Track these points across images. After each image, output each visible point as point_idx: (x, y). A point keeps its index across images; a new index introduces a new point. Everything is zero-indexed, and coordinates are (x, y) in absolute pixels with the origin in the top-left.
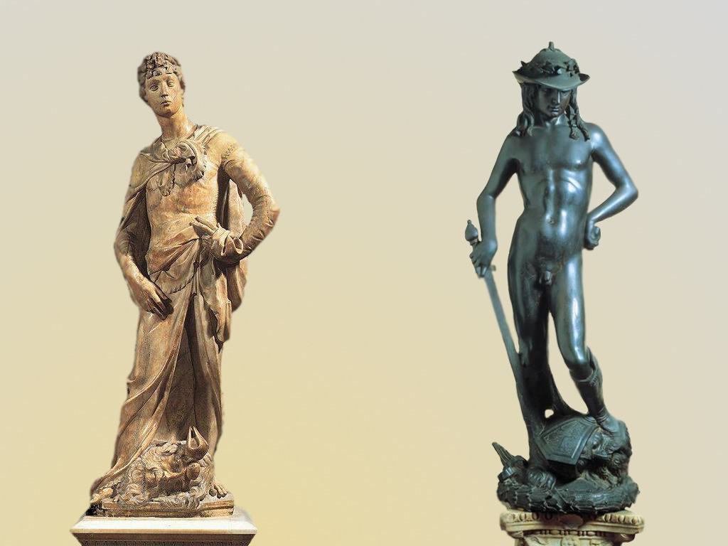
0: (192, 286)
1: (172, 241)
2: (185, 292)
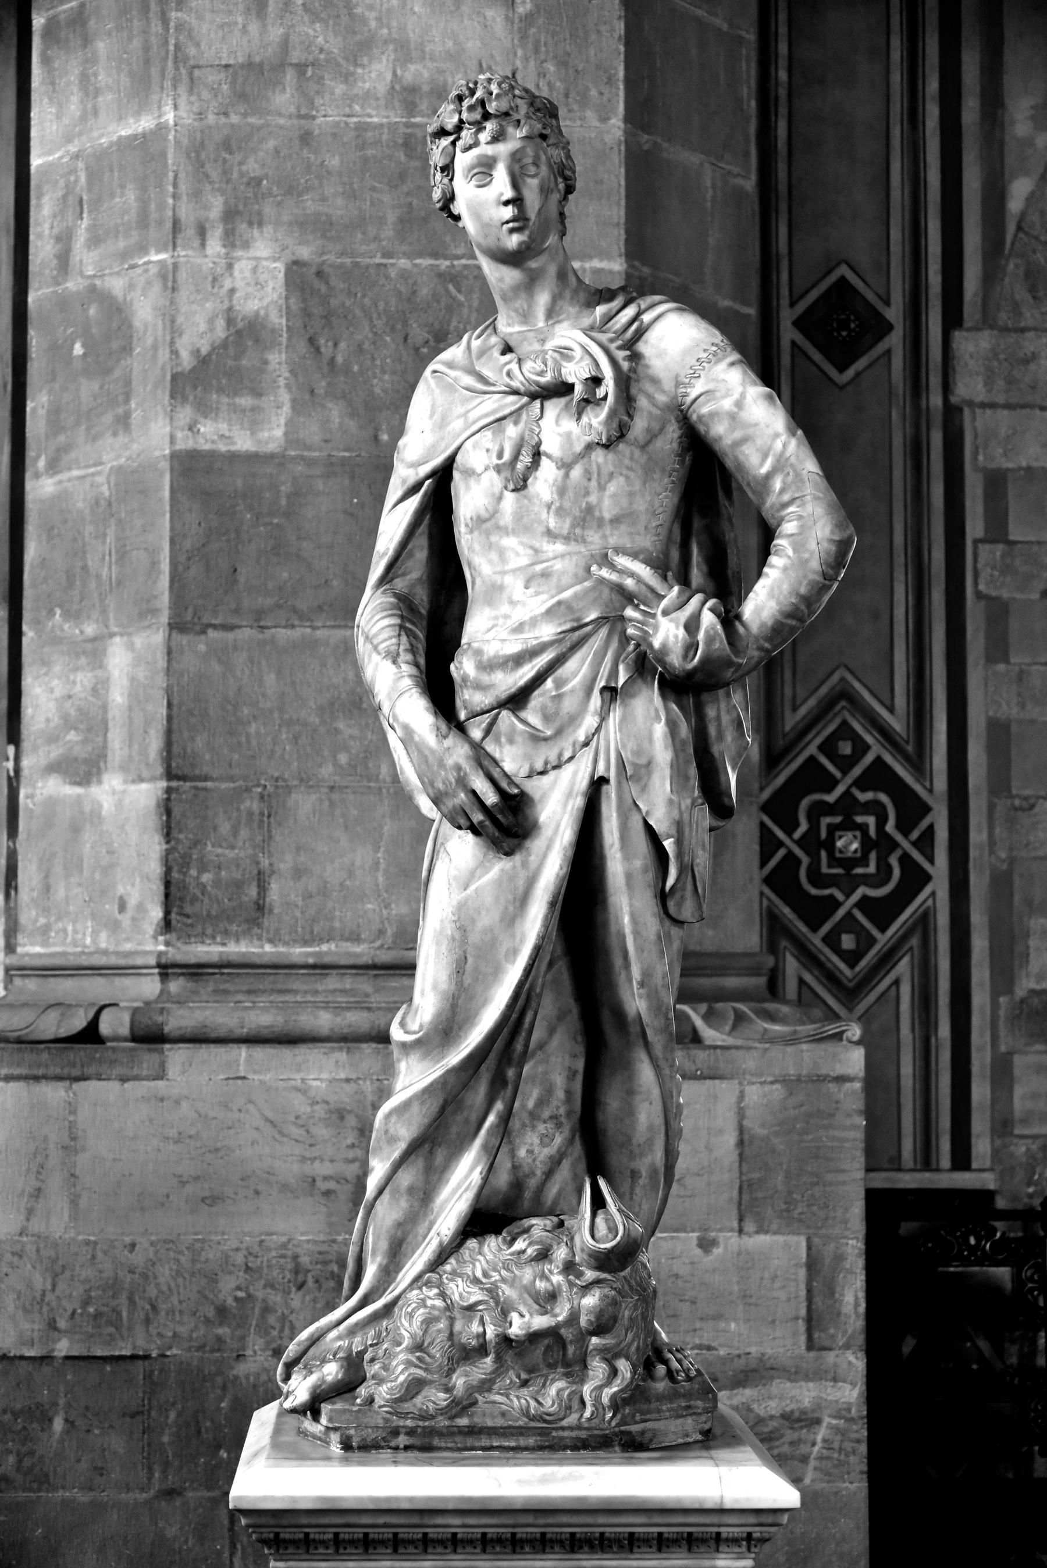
0: (596, 754)
1: (534, 622)
2: (575, 778)
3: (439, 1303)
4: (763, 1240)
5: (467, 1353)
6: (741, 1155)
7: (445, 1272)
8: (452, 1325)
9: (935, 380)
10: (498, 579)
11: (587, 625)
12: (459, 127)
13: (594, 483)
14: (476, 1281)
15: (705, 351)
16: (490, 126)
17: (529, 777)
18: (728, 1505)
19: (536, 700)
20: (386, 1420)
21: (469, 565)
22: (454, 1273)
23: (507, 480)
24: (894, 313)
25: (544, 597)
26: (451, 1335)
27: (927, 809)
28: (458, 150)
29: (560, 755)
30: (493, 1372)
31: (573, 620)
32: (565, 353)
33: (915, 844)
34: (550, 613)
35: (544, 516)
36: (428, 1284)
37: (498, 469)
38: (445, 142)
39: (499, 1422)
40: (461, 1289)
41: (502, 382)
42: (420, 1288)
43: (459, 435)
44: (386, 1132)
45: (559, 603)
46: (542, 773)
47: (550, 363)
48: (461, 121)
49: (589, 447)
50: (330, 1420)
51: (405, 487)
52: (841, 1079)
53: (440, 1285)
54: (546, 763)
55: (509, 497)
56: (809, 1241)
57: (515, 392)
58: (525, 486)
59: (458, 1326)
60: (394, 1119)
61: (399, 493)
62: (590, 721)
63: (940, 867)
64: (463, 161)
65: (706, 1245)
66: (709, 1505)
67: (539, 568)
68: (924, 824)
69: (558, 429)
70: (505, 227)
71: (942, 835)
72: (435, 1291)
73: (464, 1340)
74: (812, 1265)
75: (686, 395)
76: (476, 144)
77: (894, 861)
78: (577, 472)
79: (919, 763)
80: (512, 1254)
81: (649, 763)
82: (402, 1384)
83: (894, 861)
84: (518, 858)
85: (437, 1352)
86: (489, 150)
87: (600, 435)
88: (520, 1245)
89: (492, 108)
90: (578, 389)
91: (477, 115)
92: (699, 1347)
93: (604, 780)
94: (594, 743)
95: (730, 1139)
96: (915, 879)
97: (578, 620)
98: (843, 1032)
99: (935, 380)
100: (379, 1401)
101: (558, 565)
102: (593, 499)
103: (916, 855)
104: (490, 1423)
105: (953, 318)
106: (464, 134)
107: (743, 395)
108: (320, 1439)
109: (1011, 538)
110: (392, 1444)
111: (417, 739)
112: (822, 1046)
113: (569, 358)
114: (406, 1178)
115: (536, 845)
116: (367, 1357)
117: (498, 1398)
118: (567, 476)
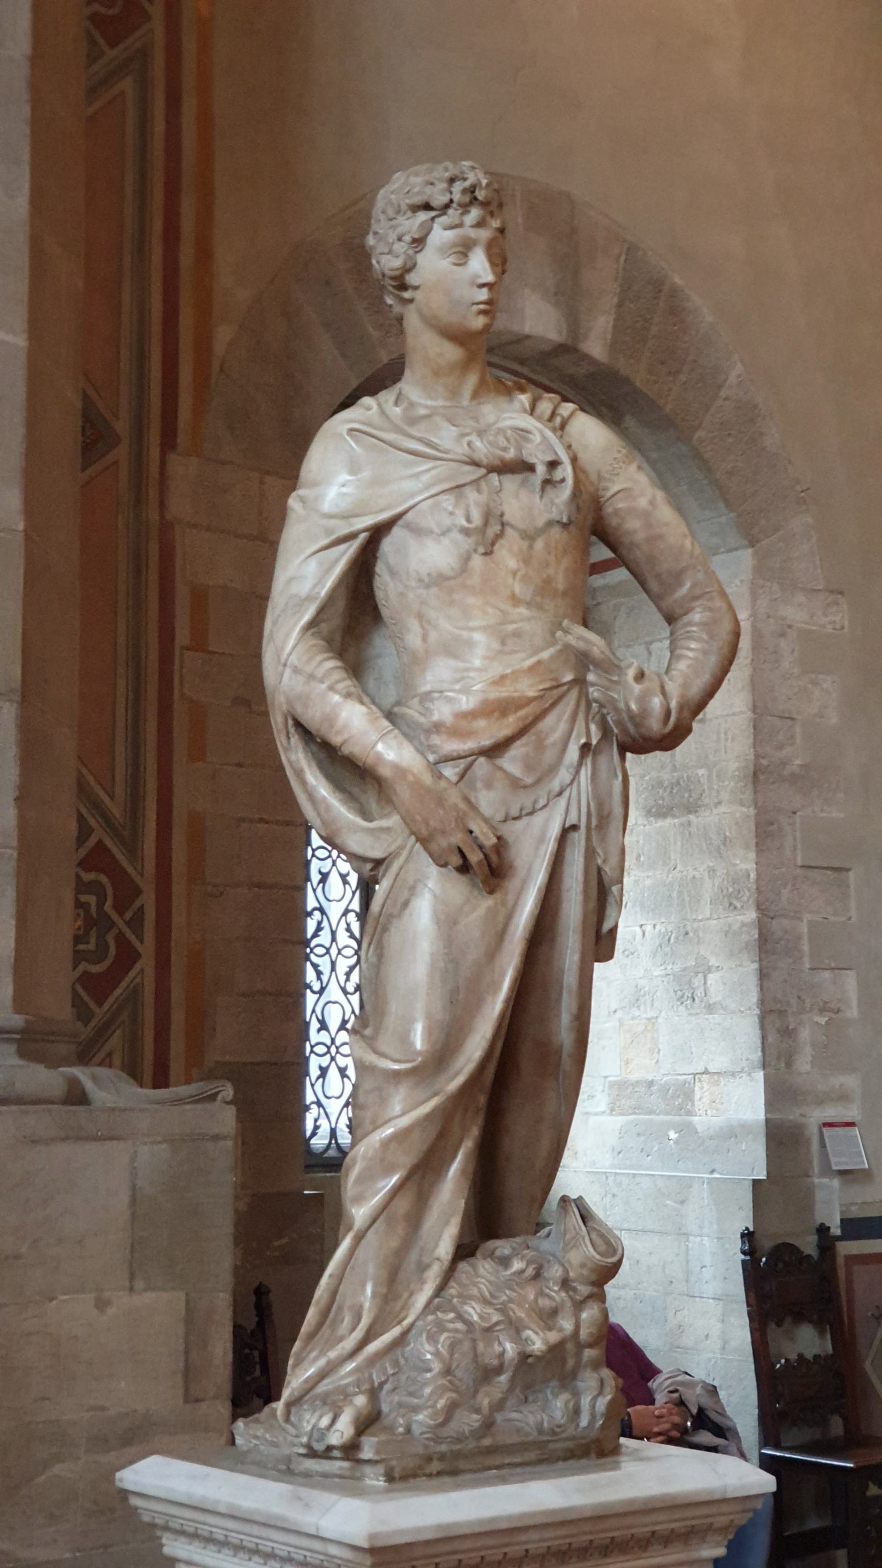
3: (459, 1326)
4: (149, 1297)
5: (487, 1374)
6: (134, 1216)
7: (453, 1297)
8: (474, 1348)
9: (153, 494)
10: (465, 634)
11: (565, 684)
12: (447, 206)
13: (552, 558)
14: (486, 1302)
15: (619, 452)
16: (475, 213)
17: (505, 821)
18: (730, 1495)
19: (518, 750)
20: (426, 1447)
21: (420, 617)
22: (465, 1298)
23: (478, 544)
24: (122, 426)
25: (522, 655)
26: (476, 1355)
27: (138, 892)
28: (437, 227)
29: (535, 802)
30: (507, 1391)
31: (551, 680)
32: (523, 433)
33: (128, 923)
34: (532, 669)
35: (510, 580)
36: (438, 1308)
37: (466, 532)
38: (423, 216)
39: (516, 1439)
40: (478, 1310)
41: (461, 450)
42: (433, 1313)
43: (413, 495)
44: (382, 1160)
45: (539, 662)
46: (515, 819)
47: (512, 441)
48: (451, 201)
49: (550, 524)
50: (378, 1452)
51: (334, 537)
52: (216, 1138)
53: (453, 1309)
54: (521, 810)
55: (477, 561)
56: (187, 1295)
57: (476, 464)
58: (491, 552)
59: (481, 1346)
60: (393, 1146)
61: (326, 541)
62: (564, 775)
63: (147, 947)
64: (440, 236)
65: (101, 1305)
66: (717, 1496)
67: (511, 628)
68: (137, 904)
69: (519, 502)
70: (475, 308)
71: (150, 915)
72: (452, 1315)
73: (487, 1361)
74: (189, 1319)
75: (606, 489)
76: (460, 225)
77: (110, 938)
78: (539, 545)
79: (132, 848)
80: (512, 1274)
81: (609, 815)
82: (442, 1408)
83: (110, 938)
84: (498, 895)
85: (464, 1374)
86: (473, 233)
87: (561, 513)
88: (517, 1265)
89: (481, 195)
90: (541, 469)
91: (467, 198)
92: (93, 1408)
93: (574, 828)
94: (566, 794)
95: (123, 1199)
96: (128, 956)
97: (556, 679)
98: (217, 1094)
99: (153, 494)
100: (416, 1430)
101: (526, 626)
102: (551, 571)
103: (129, 934)
104: (509, 1441)
105: (169, 440)
106: (450, 211)
107: (654, 497)
108: (341, 1477)
109: (210, 649)
110: (427, 1471)
111: (410, 778)
112: (199, 1106)
113: (527, 440)
114: (403, 1204)
115: (512, 885)
116: (388, 1387)
117: (514, 1415)
118: (531, 547)
